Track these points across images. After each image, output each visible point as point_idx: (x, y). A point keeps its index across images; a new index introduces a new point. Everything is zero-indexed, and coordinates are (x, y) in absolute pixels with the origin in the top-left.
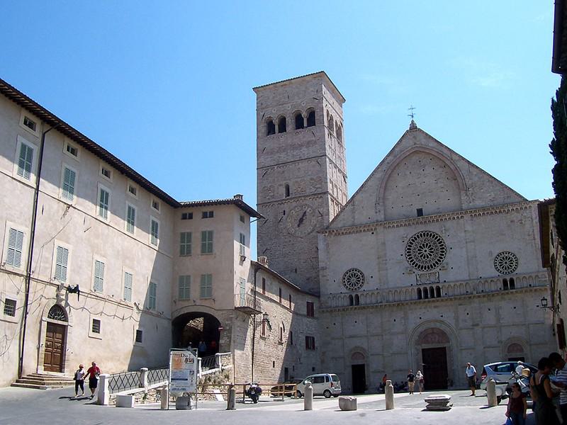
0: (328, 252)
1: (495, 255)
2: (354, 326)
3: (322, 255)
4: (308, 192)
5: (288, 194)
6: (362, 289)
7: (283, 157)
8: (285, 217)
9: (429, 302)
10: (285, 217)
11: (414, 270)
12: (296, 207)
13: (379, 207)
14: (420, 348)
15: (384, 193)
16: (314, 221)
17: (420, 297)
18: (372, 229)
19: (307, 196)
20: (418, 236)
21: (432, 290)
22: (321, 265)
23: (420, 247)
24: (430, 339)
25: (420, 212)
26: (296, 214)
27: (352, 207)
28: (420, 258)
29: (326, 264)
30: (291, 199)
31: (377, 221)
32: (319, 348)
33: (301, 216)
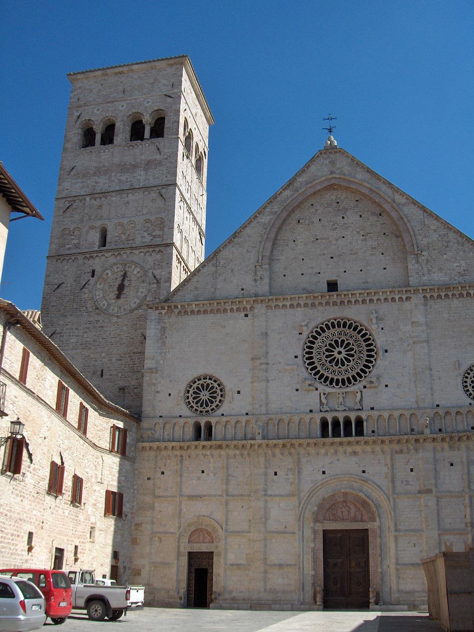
0: (164, 343)
1: (465, 367)
2: (199, 478)
3: (151, 347)
4: (138, 242)
5: (104, 242)
6: (219, 412)
7: (103, 183)
8: (93, 280)
9: (341, 444)
10: (93, 280)
11: (318, 385)
12: (115, 264)
13: (259, 273)
14: (320, 527)
15: (272, 251)
16: (143, 290)
17: (324, 434)
18: (245, 309)
19: (136, 248)
20: (327, 325)
21: (348, 422)
22: (148, 364)
23: (331, 345)
24: (340, 514)
25: (332, 286)
26: (113, 277)
27: (214, 269)
28: (328, 364)
29: (157, 362)
30: (108, 251)
31: (256, 295)
32: (129, 516)
33: (119, 281)
